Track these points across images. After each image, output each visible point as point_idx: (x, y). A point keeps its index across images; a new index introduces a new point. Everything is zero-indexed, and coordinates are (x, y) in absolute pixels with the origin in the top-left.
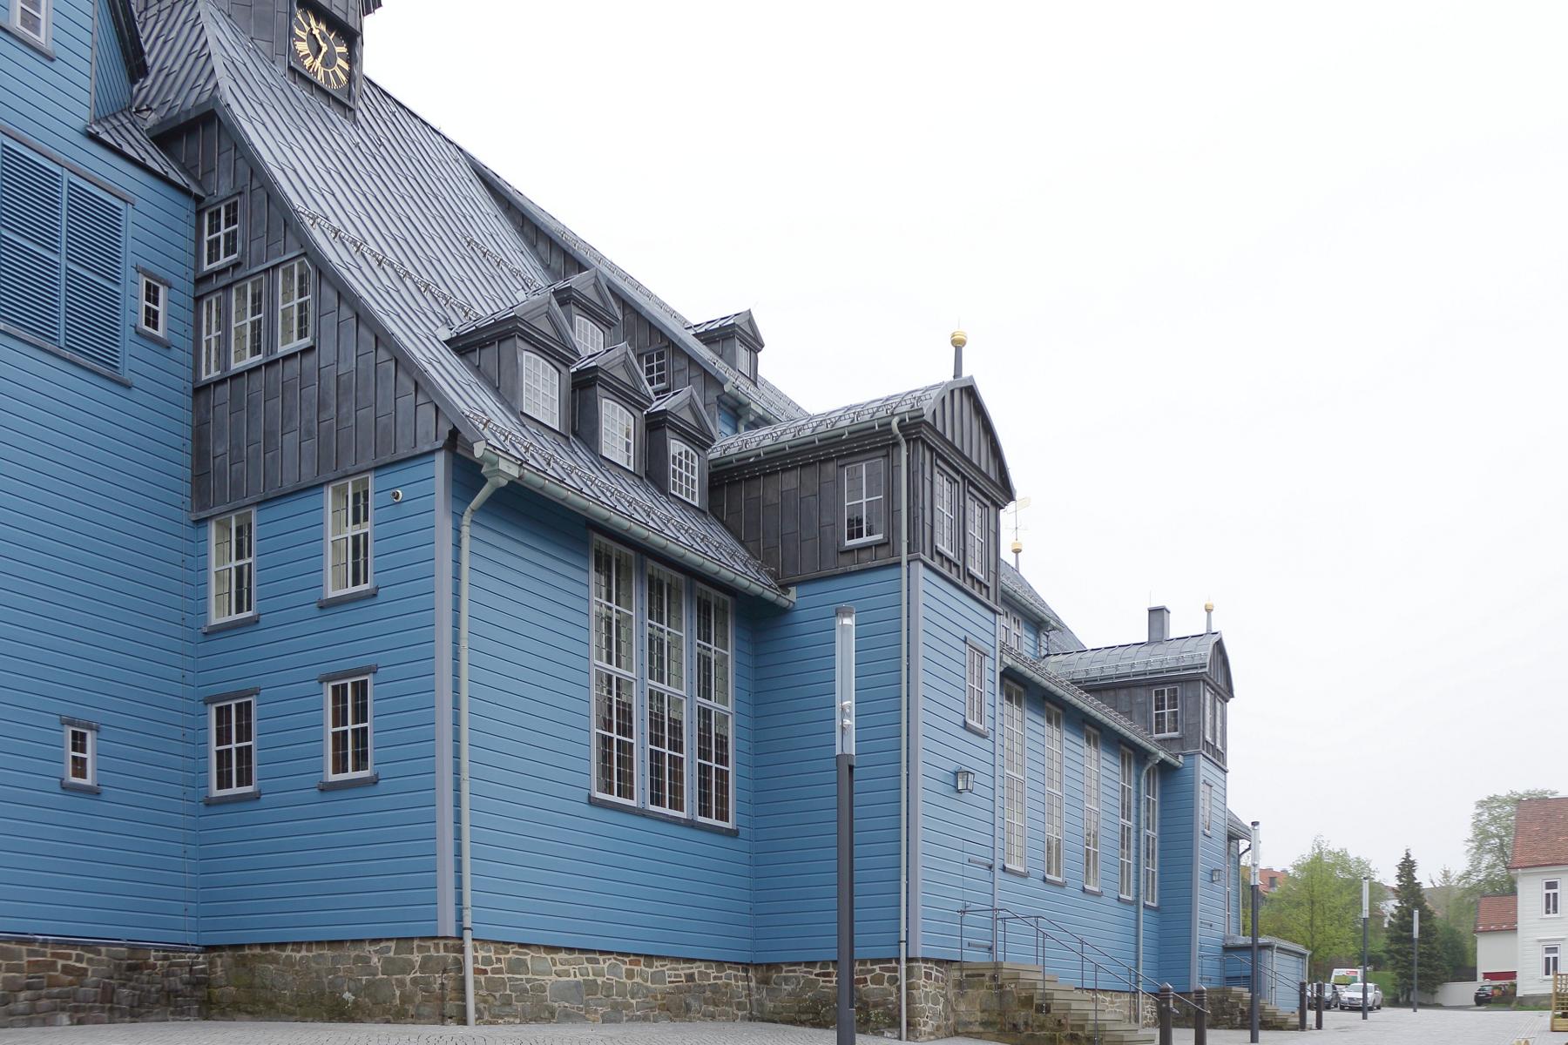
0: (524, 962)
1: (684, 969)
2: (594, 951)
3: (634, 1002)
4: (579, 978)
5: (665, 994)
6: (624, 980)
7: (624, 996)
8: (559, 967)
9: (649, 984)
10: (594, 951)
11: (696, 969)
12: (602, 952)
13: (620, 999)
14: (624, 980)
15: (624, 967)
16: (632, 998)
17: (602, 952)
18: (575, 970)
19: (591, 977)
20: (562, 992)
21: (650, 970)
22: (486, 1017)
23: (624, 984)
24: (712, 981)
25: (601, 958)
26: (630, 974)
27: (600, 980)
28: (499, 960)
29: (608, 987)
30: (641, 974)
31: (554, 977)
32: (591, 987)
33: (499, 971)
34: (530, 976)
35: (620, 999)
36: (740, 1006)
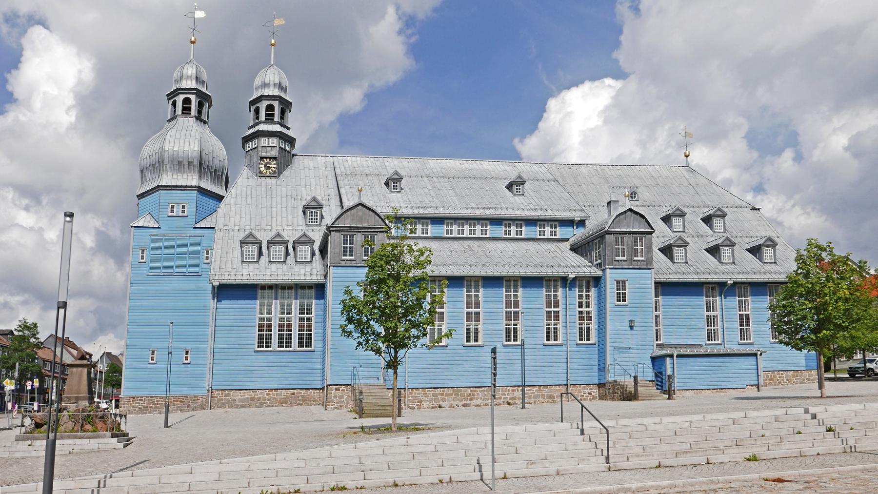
0: (230, 394)
1: (292, 391)
2: (255, 389)
3: (269, 402)
4: (249, 397)
5: (280, 399)
6: (265, 396)
7: (265, 400)
8: (242, 394)
9: (275, 397)
10: (255, 389)
11: (295, 391)
12: (258, 389)
13: (263, 401)
14: (265, 396)
15: (266, 392)
16: (268, 400)
17: (258, 389)
18: (247, 395)
19: (253, 396)
20: (241, 401)
21: (276, 393)
22: (216, 408)
23: (265, 397)
24: (303, 394)
25: (258, 391)
26: (268, 394)
27: (256, 397)
28: (222, 394)
29: (259, 399)
30: (272, 394)
31: (240, 397)
32: (253, 399)
33: (222, 396)
34: (232, 397)
35: (263, 401)
36: (314, 401)
